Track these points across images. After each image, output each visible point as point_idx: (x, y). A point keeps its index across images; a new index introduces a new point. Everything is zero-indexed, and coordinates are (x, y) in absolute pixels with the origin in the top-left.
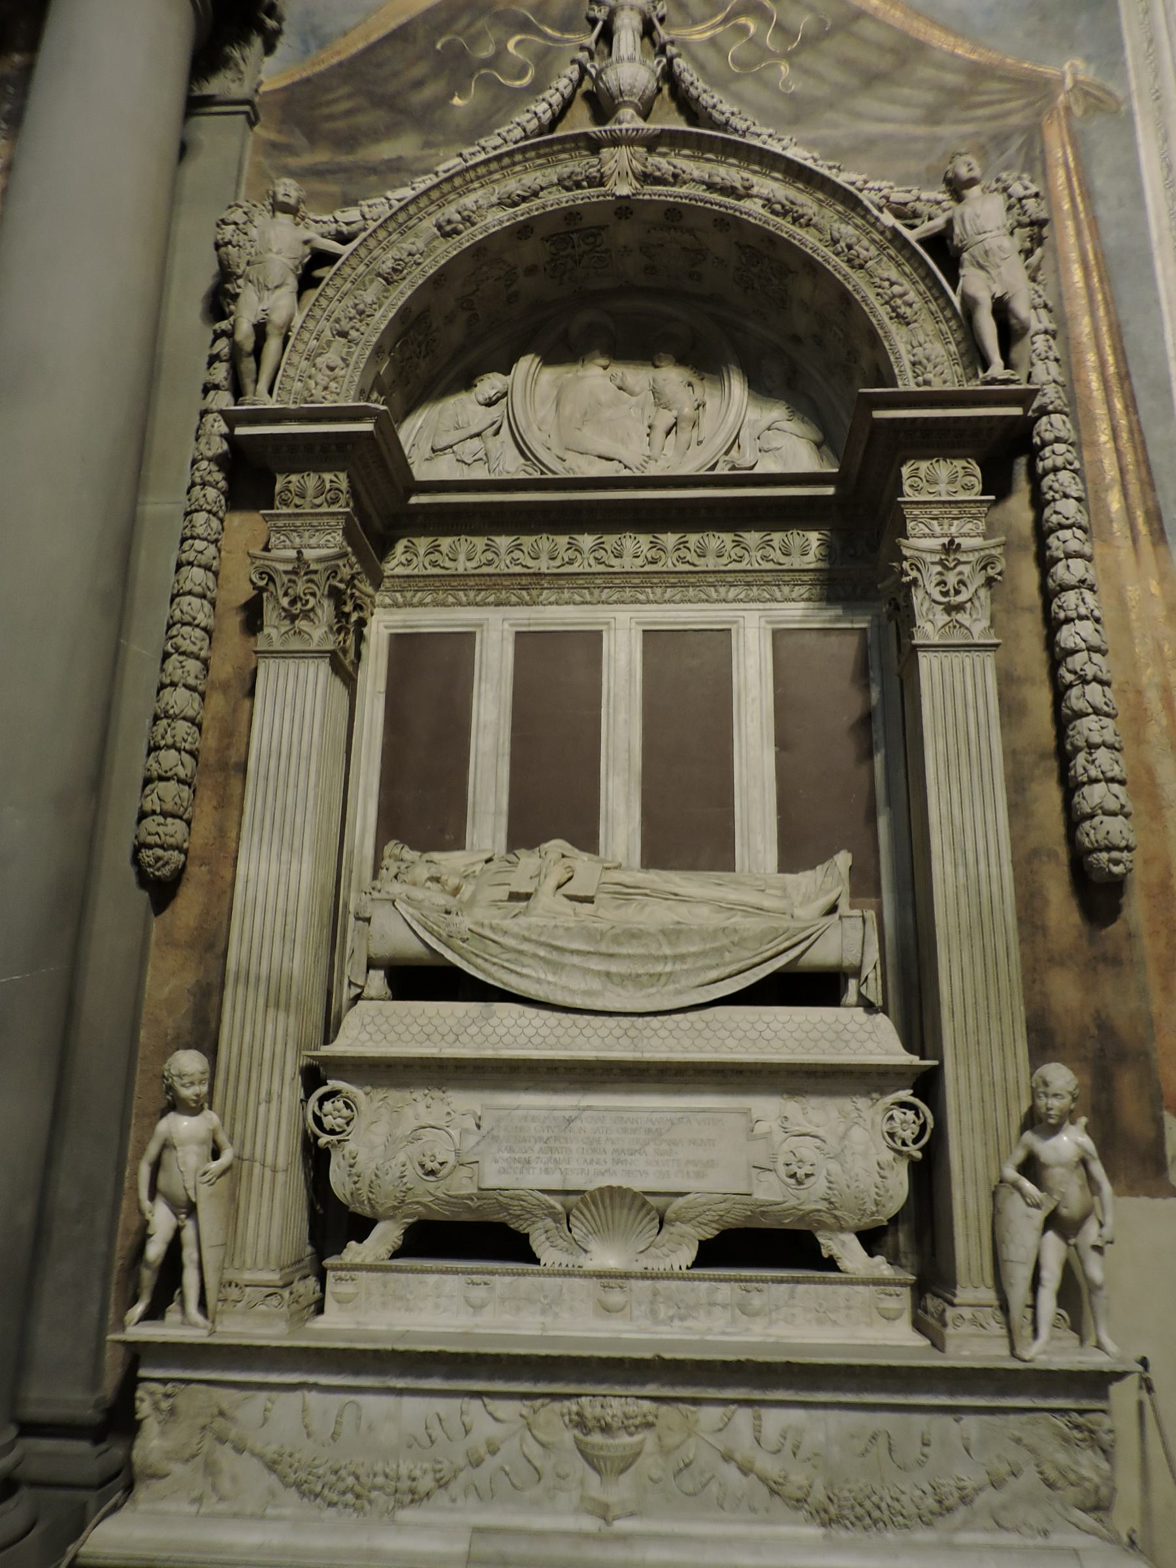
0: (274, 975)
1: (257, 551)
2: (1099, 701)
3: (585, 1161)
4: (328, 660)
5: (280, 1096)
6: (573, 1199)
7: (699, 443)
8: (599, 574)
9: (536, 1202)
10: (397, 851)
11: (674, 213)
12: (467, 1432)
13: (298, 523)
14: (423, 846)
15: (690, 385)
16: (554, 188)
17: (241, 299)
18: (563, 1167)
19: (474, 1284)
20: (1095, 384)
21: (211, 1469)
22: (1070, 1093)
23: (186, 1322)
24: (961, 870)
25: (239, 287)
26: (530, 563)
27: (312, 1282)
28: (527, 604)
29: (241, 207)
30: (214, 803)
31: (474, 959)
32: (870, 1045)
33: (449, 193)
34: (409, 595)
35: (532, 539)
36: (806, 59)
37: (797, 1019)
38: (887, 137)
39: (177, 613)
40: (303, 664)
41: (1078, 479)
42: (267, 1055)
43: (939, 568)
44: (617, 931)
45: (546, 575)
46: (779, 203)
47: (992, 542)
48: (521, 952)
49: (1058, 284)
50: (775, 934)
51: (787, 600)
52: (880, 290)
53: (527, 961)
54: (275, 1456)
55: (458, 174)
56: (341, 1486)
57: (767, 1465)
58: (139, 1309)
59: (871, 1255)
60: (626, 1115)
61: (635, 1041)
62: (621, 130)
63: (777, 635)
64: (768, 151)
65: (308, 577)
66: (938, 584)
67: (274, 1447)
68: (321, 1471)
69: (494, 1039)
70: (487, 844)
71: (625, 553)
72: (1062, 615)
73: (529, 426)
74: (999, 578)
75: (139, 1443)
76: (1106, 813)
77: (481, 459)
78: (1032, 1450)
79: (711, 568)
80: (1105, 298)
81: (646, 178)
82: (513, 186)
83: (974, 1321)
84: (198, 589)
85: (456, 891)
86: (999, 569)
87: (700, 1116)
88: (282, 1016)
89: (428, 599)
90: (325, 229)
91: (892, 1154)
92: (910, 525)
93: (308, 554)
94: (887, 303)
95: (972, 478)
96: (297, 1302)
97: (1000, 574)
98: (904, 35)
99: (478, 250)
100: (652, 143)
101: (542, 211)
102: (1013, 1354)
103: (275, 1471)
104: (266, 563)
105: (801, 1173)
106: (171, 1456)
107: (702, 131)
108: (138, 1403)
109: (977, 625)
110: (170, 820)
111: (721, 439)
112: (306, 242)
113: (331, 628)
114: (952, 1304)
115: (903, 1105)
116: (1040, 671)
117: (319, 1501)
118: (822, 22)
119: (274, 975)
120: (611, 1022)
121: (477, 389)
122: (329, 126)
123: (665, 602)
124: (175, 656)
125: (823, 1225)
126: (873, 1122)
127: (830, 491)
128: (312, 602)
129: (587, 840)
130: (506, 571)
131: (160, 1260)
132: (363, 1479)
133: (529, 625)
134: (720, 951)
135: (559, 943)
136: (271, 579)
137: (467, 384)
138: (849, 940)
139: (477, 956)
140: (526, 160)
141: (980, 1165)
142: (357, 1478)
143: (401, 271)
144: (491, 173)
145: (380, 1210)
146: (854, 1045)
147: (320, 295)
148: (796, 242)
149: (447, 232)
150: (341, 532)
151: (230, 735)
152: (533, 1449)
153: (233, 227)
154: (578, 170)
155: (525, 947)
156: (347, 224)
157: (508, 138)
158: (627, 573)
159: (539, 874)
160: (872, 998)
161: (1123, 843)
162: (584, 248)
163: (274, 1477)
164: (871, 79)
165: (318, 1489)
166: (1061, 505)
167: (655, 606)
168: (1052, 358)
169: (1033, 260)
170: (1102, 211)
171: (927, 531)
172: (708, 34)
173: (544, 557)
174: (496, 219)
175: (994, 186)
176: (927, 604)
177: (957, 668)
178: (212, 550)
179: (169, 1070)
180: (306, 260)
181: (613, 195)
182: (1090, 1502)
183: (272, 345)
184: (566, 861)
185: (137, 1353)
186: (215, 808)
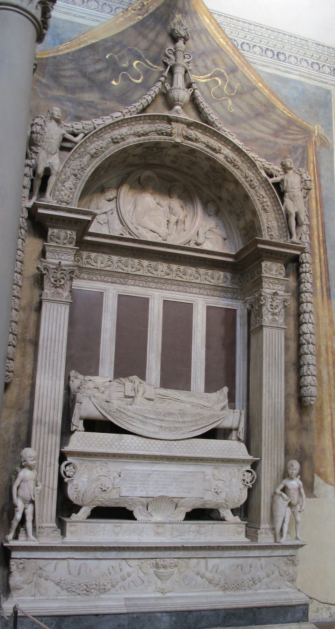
2: (312, 351)
5: (54, 465)
6: (149, 499)
9: (138, 500)
11: (192, 151)
12: (121, 570)
13: (58, 249)
14: (85, 373)
16: (153, 133)
18: (147, 489)
19: (116, 526)
20: (316, 243)
21: (37, 586)
24: (270, 399)
25: (38, 150)
26: (125, 268)
28: (123, 284)
30: (21, 354)
32: (239, 453)
33: (116, 126)
36: (237, 100)
38: (262, 139)
40: (60, 305)
42: (49, 450)
43: (270, 300)
44: (165, 412)
45: (131, 274)
48: (133, 418)
51: (212, 296)
54: (59, 581)
56: (82, 588)
59: (235, 516)
62: (180, 118)
64: (228, 139)
65: (61, 272)
69: (123, 447)
70: (107, 374)
72: (304, 321)
76: (311, 385)
78: (278, 567)
80: (321, 213)
81: (187, 138)
85: (103, 393)
87: (190, 474)
88: (54, 436)
90: (68, 129)
92: (264, 284)
93: (63, 263)
98: (268, 101)
99: (124, 150)
100: (189, 125)
102: (275, 542)
104: (47, 264)
105: (219, 492)
106: (23, 583)
107: (205, 124)
108: (12, 566)
110: (10, 361)
111: (194, 231)
112: (63, 135)
114: (259, 529)
115: (248, 471)
117: (74, 593)
121: (106, 194)
122: (63, 80)
126: (238, 476)
132: (89, 586)
135: (146, 415)
136: (48, 270)
138: (234, 419)
140: (145, 120)
141: (269, 489)
144: (132, 122)
145: (85, 503)
149: (115, 142)
151: (26, 328)
152: (141, 575)
154: (163, 129)
155: (134, 416)
156: (77, 129)
160: (241, 438)
163: (59, 587)
164: (258, 115)
165: (74, 590)
166: (306, 284)
170: (322, 182)
171: (268, 287)
172: (205, 81)
173: (130, 266)
174: (133, 141)
175: (297, 172)
176: (267, 311)
179: (26, 455)
182: (291, 580)
186: (21, 356)
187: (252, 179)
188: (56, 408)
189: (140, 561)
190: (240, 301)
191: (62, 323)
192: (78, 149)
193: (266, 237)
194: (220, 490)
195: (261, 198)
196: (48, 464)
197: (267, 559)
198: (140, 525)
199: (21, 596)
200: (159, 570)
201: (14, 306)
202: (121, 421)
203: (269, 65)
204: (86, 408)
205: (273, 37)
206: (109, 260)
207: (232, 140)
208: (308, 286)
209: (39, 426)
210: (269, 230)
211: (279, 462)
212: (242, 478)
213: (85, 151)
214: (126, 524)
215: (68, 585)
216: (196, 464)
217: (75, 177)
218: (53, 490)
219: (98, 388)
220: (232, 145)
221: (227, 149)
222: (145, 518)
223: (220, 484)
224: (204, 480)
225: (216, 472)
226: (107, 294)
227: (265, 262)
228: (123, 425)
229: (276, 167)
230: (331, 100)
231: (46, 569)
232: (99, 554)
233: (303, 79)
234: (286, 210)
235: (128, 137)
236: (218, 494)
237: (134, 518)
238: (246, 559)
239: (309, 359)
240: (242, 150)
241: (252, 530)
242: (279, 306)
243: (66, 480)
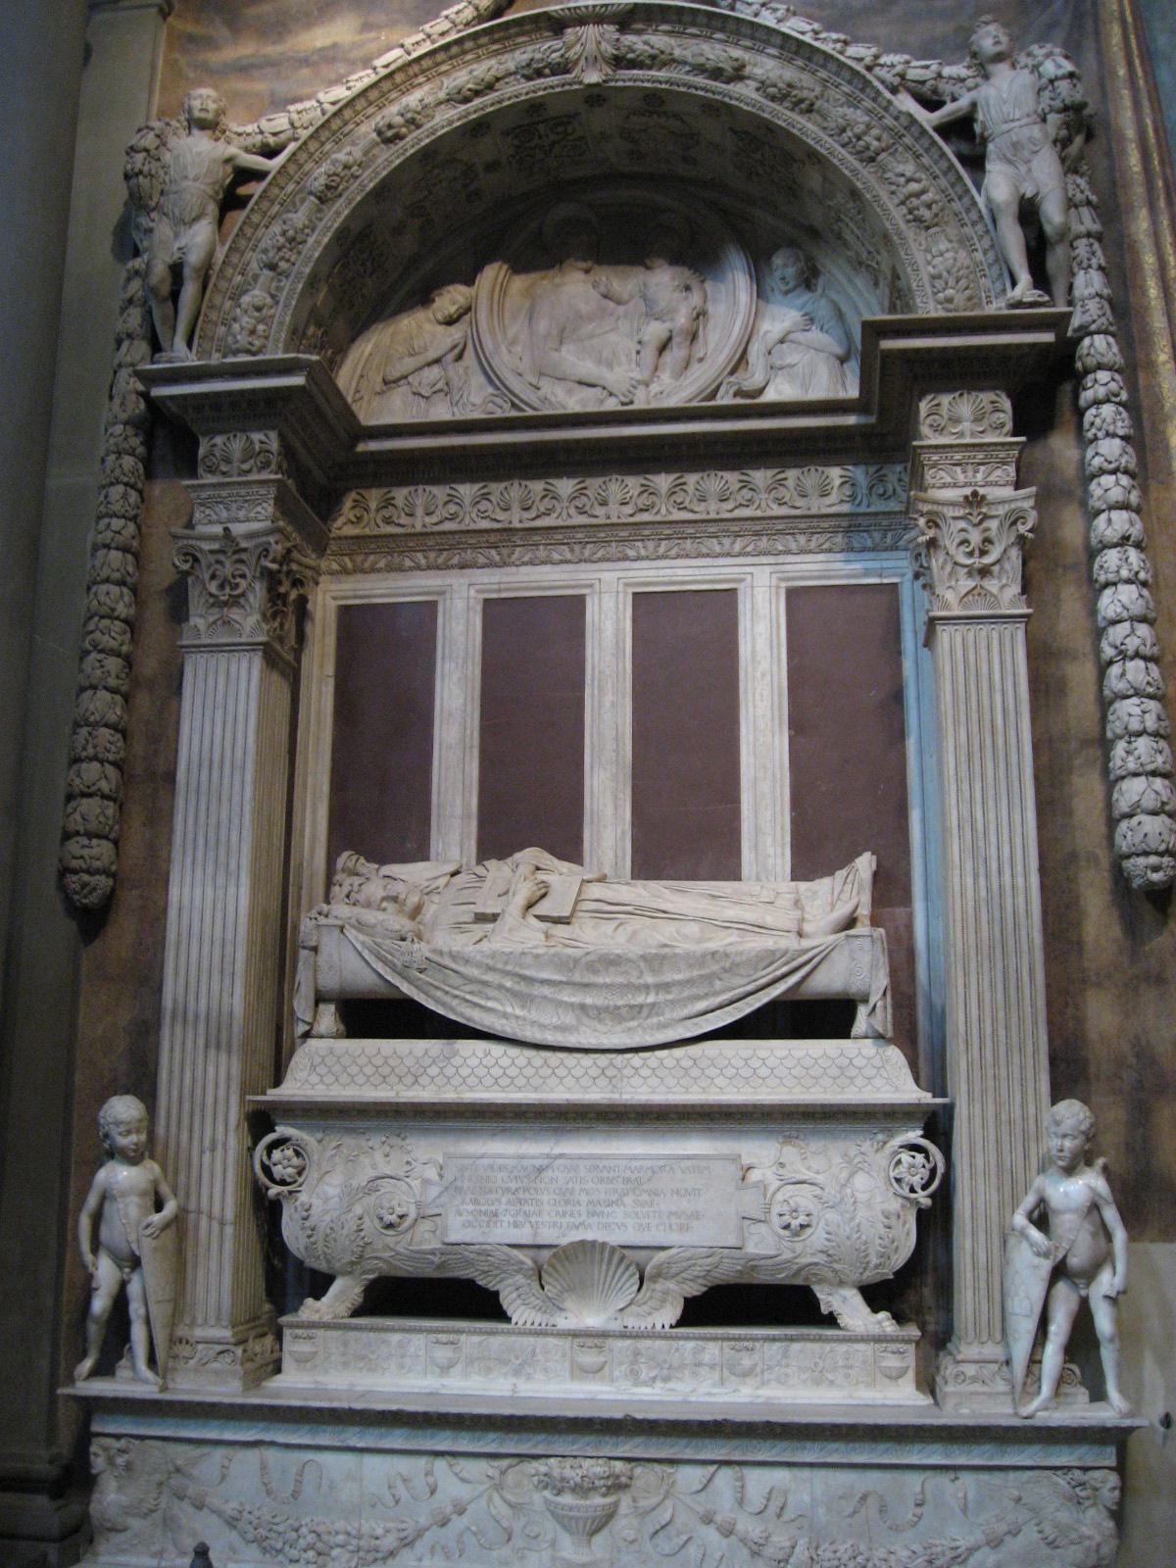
0: (214, 1014)
1: (180, 531)
3: (557, 1213)
4: (260, 653)
5: (225, 1145)
6: (546, 1254)
7: (701, 360)
8: (580, 526)
10: (350, 864)
11: (654, 100)
13: (224, 493)
14: (381, 855)
15: (688, 288)
17: (157, 233)
22: (1083, 1133)
23: (137, 1379)
24: (982, 881)
26: (501, 516)
27: (269, 1340)
29: (153, 129)
31: (433, 992)
34: (359, 559)
35: (502, 486)
37: (798, 1054)
39: (95, 602)
41: (1125, 414)
42: (210, 1100)
43: (962, 524)
44: (592, 957)
46: (775, 86)
47: (1022, 492)
48: (485, 983)
49: (1112, 169)
50: (770, 957)
51: (802, 552)
52: (894, 188)
53: (491, 992)
54: (235, 1514)
55: (400, 69)
56: (302, 1543)
58: (88, 1364)
60: (601, 1163)
61: (614, 1081)
63: (793, 595)
65: (236, 557)
66: (962, 543)
67: (234, 1504)
68: (281, 1528)
71: (611, 499)
73: (497, 347)
74: (1030, 535)
75: (95, 1496)
77: (441, 390)
79: (713, 516)
81: (619, 62)
82: (462, 78)
83: (974, 1379)
84: (117, 576)
86: (1029, 525)
87: (689, 1163)
89: (382, 564)
90: (250, 141)
91: (900, 1201)
92: (929, 474)
93: (238, 529)
94: (903, 203)
95: (1002, 415)
96: (252, 1360)
97: (1030, 531)
101: (497, 107)
103: (235, 1527)
104: (191, 542)
106: (128, 1510)
108: (92, 1457)
109: (1006, 592)
110: (95, 841)
112: (229, 160)
113: (264, 615)
115: (914, 1148)
116: (1082, 643)
117: (280, 1557)
119: (214, 1014)
120: (587, 1060)
123: (658, 558)
124: (94, 655)
125: (822, 1281)
127: (851, 420)
128: (243, 584)
129: (568, 846)
130: (472, 526)
131: (106, 1315)
132: (325, 1537)
133: (500, 591)
134: (709, 978)
135: (527, 973)
136: (196, 560)
137: (423, 297)
139: (437, 988)
140: (479, 47)
143: (336, 188)
144: (438, 65)
145: (337, 1265)
146: (859, 1081)
147: (244, 223)
148: (795, 131)
149: (389, 137)
150: (272, 502)
152: (505, 1510)
153: (144, 154)
154: (538, 56)
155: (489, 977)
156: (275, 134)
157: (458, 21)
158: (613, 525)
159: (506, 893)
160: (881, 1030)
161: (1162, 847)
162: (552, 137)
163: (234, 1533)
165: (279, 1545)
168: (1095, 266)
174: (447, 118)
176: (948, 568)
177: (984, 644)
178: (132, 527)
180: (228, 181)
181: (581, 83)
183: (189, 291)
184: (541, 876)
185: (92, 1406)
188: (228, 968)
191: (241, 709)
192: (276, 191)
194: (802, 1219)
195: (898, 183)
197: (984, 1477)
199: (123, 1551)
200: (559, 1499)
201: (101, 679)
202: (447, 999)
209: (178, 1030)
210: (939, 284)
212: (892, 1174)
213: (301, 191)
214: (472, 1336)
215: (260, 1530)
216: (711, 1130)
217: (271, 274)
219: (395, 899)
220: (778, 41)
221: (765, 59)
222: (538, 1318)
225: (790, 1153)
226: (448, 602)
227: (929, 397)
228: (452, 1010)
231: (195, 1472)
232: (353, 1437)
235: (430, 112)
236: (797, 1234)
238: (897, 1474)
239: (1129, 713)
240: (810, 46)
242: (995, 540)
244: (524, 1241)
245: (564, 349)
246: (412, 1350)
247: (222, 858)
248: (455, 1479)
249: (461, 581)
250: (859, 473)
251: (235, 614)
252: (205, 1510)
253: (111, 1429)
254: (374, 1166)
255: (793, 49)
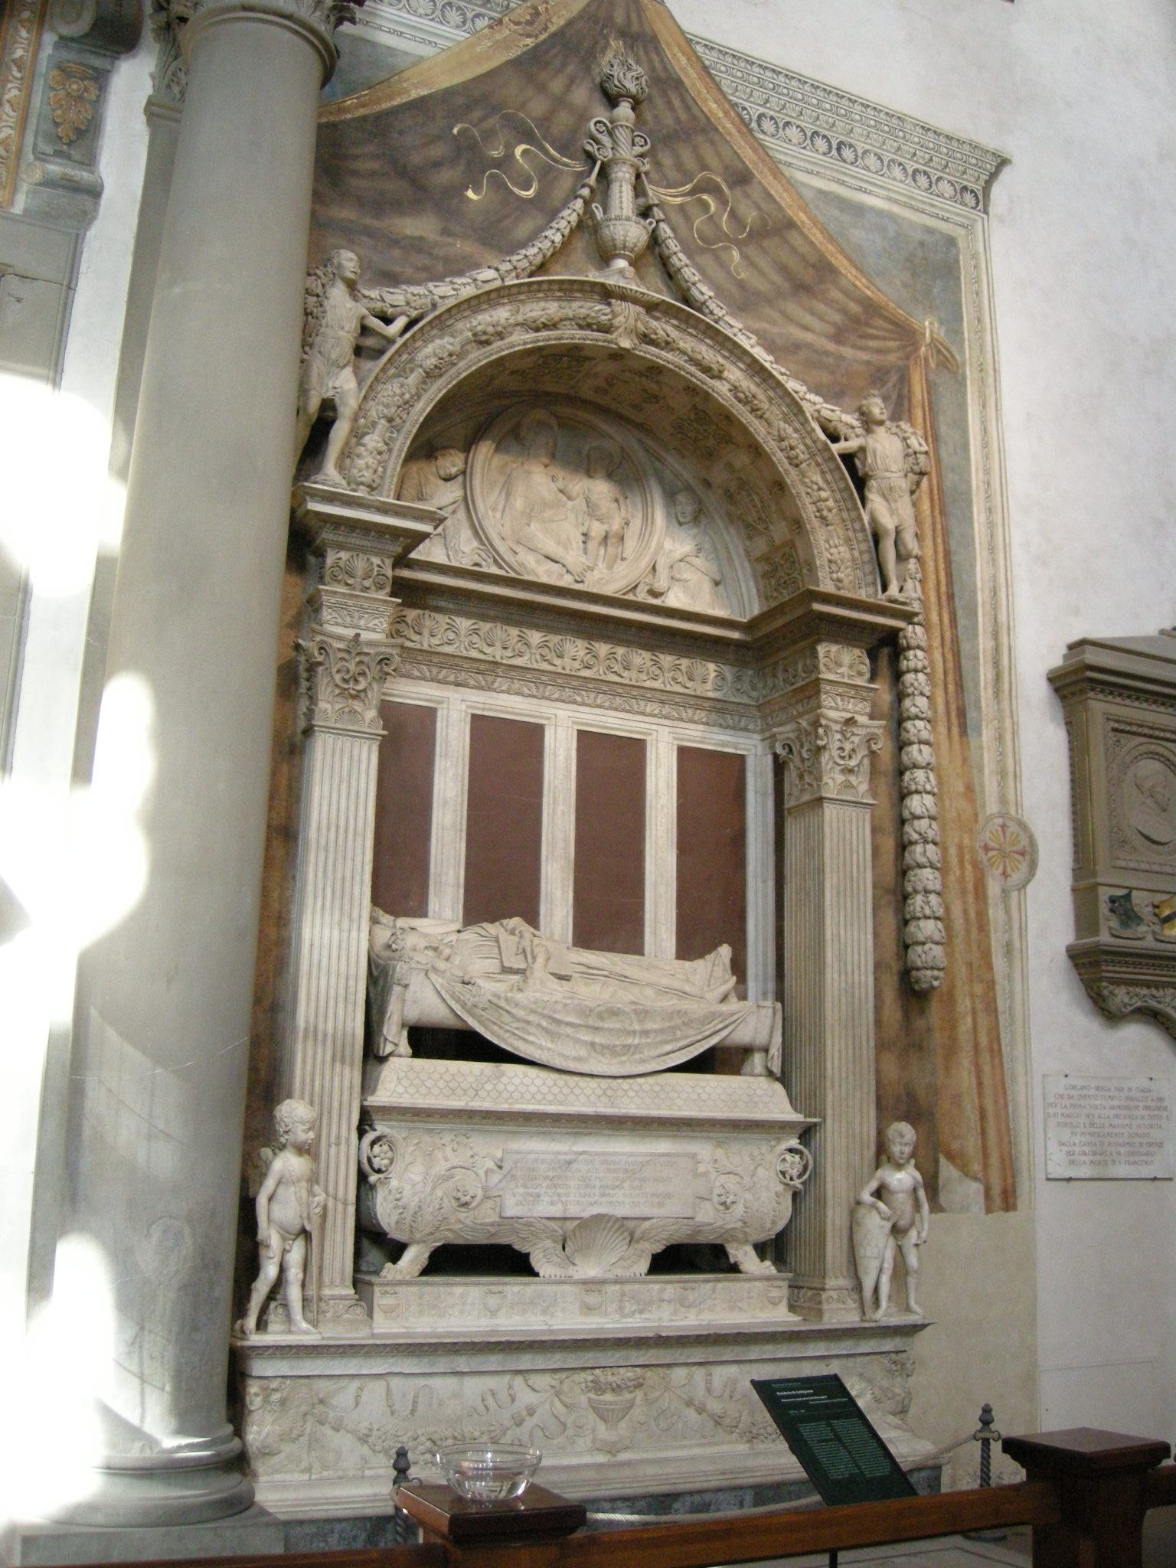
0: (340, 1033)
5: (348, 1140)
7: (623, 559)
11: (655, 370)
14: (396, 913)
15: (616, 500)
21: (314, 1442)
28: (481, 688)
36: (752, 251)
38: (809, 346)
42: (336, 1104)
43: (838, 736)
44: (601, 1008)
48: (528, 1022)
51: (691, 721)
53: (532, 1030)
54: (366, 1431)
56: (421, 1448)
57: (715, 1406)
60: (610, 1159)
67: (365, 1424)
69: (505, 1095)
70: (448, 913)
78: (869, 1381)
79: (633, 683)
81: (646, 339)
83: (839, 1300)
85: (447, 959)
87: (664, 1159)
88: (347, 1070)
98: (822, 257)
100: (651, 307)
105: (729, 1201)
107: (684, 308)
111: (645, 562)
114: (824, 1289)
115: (791, 1150)
118: (763, 219)
119: (340, 1033)
120: (593, 1083)
125: (736, 1240)
127: (735, 635)
134: (674, 1028)
135: (558, 1016)
138: (755, 1022)
142: (434, 1442)
152: (560, 1409)
164: (801, 288)
167: (587, 709)
169: (914, 497)
170: (944, 454)
176: (831, 764)
187: (794, 443)
188: (351, 998)
189: (557, 1376)
190: (755, 736)
191: (363, 785)
193: (827, 586)
194: (731, 1198)
195: (814, 490)
196: (333, 1139)
197: (844, 1361)
198: (549, 1289)
199: (277, 1472)
202: (501, 1032)
203: (822, 170)
204: (421, 999)
205: (828, 107)
206: (450, 628)
207: (748, 348)
208: (922, 702)
211: (865, 1129)
214: (514, 1287)
218: (345, 1204)
219: (435, 949)
220: (749, 360)
223: (731, 1182)
224: (696, 1175)
227: (824, 644)
228: (504, 1040)
229: (844, 418)
230: (957, 262)
231: (334, 1402)
232: (462, 1363)
233: (896, 209)
234: (874, 521)
237: (532, 1273)
241: (804, 1292)
243: (373, 1178)
244: (558, 1215)
245: (533, 527)
246: (470, 1300)
247: (347, 907)
248: (528, 1390)
249: (457, 696)
250: (728, 671)
251: (357, 705)
252: (342, 1432)
253: (269, 1373)
254: (446, 1159)
255: (756, 369)
